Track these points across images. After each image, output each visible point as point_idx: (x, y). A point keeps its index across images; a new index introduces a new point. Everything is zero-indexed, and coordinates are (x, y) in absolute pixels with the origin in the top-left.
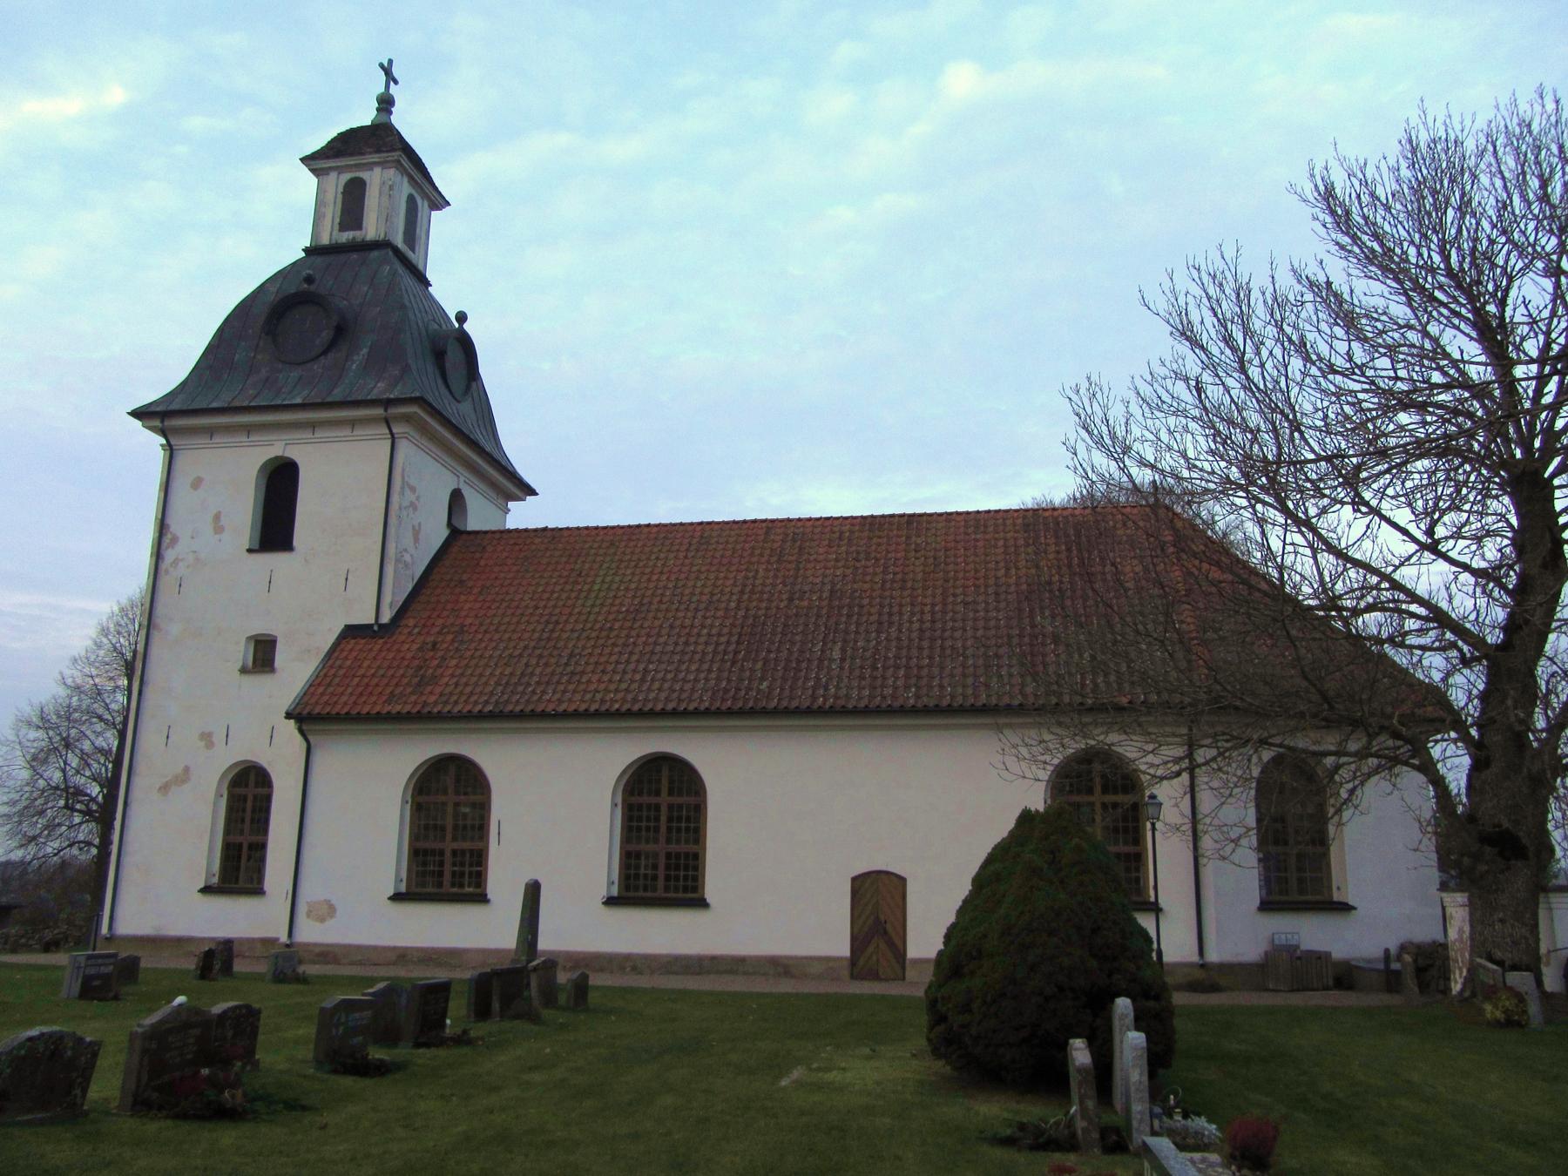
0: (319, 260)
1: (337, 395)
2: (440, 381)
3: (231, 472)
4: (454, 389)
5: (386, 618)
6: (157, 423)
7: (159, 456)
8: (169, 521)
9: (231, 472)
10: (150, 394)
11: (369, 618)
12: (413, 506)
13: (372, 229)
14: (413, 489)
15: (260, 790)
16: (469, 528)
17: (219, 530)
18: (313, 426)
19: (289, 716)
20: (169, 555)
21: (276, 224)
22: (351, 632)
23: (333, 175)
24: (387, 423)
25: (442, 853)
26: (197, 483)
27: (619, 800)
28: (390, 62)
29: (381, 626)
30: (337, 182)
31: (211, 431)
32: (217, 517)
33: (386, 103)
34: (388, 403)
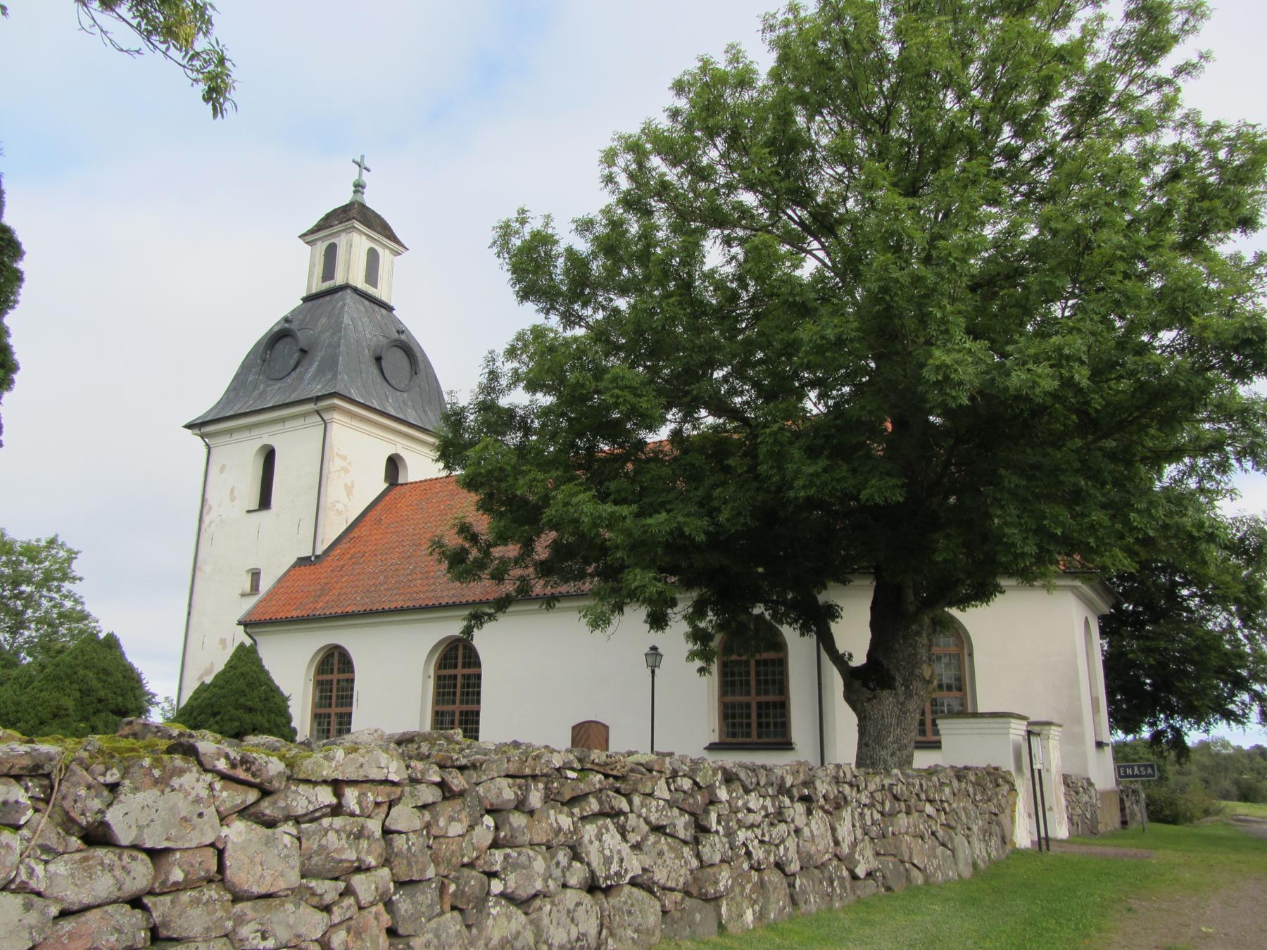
0: (309, 304)
1: (293, 398)
2: (379, 379)
3: (240, 457)
4: (393, 382)
5: (319, 552)
6: (197, 431)
7: (205, 451)
8: (208, 496)
9: (240, 457)
10: (198, 411)
11: (307, 552)
12: (346, 471)
13: (339, 280)
14: (344, 458)
15: (342, 676)
16: (410, 480)
17: (233, 499)
18: (283, 420)
19: (240, 623)
20: (207, 519)
21: (279, 284)
22: (303, 561)
23: (319, 243)
24: (318, 412)
25: (329, 716)
26: (222, 470)
27: (432, 675)
28: (362, 157)
29: (317, 557)
30: (321, 247)
31: (230, 432)
32: (232, 491)
33: (359, 187)
34: (318, 399)
